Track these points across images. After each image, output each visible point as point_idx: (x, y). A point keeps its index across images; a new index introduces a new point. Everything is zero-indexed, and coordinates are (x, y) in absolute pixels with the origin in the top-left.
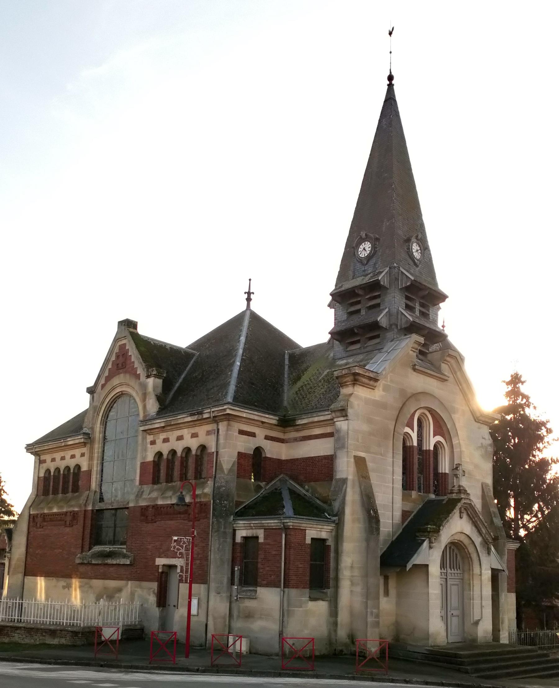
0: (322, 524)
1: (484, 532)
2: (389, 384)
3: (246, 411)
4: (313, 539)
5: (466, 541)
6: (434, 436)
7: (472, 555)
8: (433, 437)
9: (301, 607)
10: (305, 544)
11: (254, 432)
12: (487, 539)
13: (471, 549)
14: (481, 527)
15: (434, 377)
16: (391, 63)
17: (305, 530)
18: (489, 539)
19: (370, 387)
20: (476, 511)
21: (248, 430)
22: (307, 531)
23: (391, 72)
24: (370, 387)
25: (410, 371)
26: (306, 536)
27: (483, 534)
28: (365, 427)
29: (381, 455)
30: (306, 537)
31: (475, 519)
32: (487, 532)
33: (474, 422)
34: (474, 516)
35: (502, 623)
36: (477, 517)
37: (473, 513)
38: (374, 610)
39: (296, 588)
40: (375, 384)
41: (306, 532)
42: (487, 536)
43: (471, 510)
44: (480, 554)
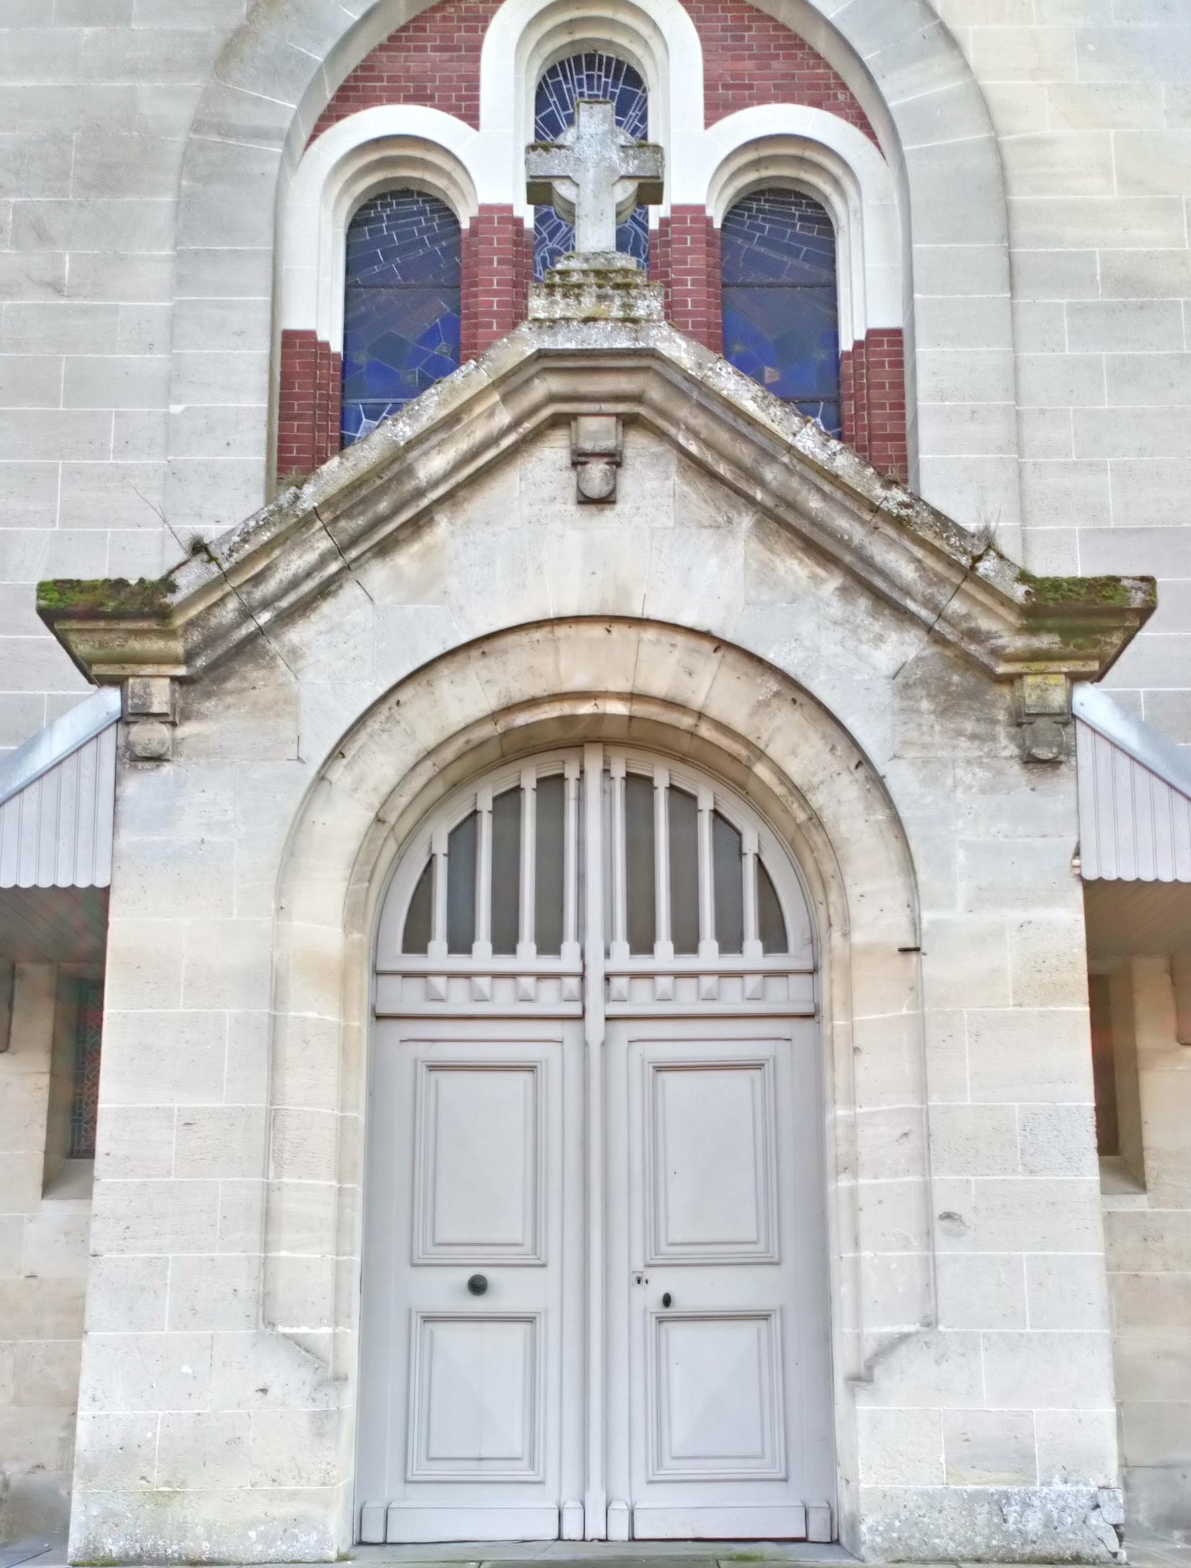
1: (907, 572)
6: (715, 109)
8: (707, 125)
12: (974, 635)
18: (985, 624)
20: (739, 413)
27: (907, 593)
31: (761, 482)
32: (930, 562)
34: (745, 453)
36: (773, 458)
37: (723, 437)
42: (956, 606)
43: (684, 412)
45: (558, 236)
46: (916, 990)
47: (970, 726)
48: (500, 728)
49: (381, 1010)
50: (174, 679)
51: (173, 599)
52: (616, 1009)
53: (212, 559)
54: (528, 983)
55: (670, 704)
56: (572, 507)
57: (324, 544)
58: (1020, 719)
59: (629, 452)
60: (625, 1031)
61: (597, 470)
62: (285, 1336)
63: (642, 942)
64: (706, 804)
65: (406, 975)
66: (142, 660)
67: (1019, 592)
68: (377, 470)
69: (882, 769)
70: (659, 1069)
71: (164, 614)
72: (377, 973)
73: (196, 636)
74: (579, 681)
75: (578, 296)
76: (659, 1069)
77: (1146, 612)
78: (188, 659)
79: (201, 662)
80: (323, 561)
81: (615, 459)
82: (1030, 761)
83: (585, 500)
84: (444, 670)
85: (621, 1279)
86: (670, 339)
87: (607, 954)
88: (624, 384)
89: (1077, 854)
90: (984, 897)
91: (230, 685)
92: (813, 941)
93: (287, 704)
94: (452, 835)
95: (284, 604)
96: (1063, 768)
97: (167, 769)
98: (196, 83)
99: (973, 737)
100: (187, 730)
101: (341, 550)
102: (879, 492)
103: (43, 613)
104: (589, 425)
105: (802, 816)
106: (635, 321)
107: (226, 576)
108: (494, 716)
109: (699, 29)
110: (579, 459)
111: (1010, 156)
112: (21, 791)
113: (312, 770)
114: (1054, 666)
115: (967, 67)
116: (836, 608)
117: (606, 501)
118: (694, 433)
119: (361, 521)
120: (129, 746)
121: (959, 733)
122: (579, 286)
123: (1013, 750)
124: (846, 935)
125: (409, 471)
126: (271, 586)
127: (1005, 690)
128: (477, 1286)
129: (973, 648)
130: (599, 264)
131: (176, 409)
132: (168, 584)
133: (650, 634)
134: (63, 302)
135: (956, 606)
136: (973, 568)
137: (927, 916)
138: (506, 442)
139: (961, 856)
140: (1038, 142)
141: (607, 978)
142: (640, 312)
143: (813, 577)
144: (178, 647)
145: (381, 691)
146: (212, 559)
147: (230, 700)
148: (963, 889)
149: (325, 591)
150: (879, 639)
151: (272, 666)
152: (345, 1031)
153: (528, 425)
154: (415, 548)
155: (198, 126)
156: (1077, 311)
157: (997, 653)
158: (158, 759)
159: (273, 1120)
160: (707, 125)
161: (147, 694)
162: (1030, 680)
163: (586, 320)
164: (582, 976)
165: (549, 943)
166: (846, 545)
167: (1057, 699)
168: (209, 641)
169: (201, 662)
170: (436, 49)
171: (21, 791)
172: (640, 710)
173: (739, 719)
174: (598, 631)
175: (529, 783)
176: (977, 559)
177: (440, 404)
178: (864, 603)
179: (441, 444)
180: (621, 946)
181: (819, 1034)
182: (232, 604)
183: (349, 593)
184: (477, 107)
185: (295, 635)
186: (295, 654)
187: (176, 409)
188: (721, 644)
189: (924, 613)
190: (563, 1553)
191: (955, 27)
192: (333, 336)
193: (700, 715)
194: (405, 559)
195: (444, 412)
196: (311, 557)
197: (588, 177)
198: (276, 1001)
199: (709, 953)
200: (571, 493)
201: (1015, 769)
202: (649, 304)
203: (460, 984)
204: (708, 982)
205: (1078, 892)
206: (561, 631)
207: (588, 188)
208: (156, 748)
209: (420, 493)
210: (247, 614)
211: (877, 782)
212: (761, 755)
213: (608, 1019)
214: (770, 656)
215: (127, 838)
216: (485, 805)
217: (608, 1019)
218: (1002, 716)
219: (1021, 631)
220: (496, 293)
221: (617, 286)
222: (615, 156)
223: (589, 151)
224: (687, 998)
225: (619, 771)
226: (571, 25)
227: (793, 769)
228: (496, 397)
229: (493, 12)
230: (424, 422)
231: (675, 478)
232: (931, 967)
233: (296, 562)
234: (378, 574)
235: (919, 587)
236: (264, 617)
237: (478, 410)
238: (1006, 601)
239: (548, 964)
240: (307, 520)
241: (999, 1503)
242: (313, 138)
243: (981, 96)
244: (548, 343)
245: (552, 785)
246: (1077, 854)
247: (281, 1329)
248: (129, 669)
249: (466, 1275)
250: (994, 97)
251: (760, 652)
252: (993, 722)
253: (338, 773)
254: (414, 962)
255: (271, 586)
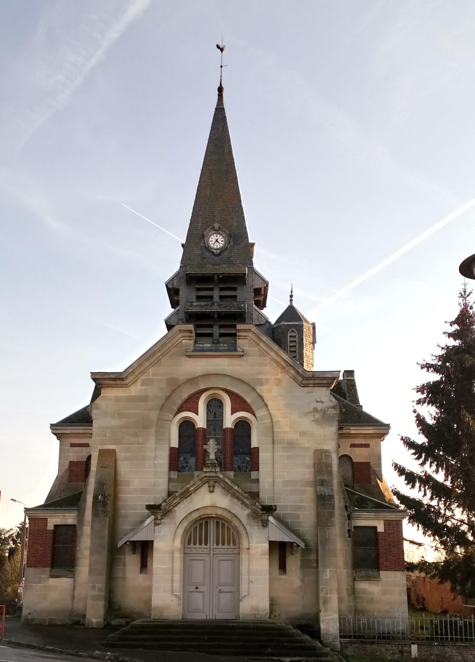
0: (64, 512)
1: (248, 503)
2: (151, 377)
3: (69, 428)
4: (56, 526)
5: (226, 514)
6: (233, 413)
7: (239, 528)
8: (231, 415)
9: (40, 582)
10: (46, 530)
11: (87, 443)
12: (256, 511)
13: (235, 522)
14: (243, 498)
15: (222, 357)
16: (221, 76)
17: (47, 519)
18: (257, 510)
19: (118, 386)
21: (81, 442)
22: (48, 519)
23: (221, 84)
24: (118, 386)
25: (184, 358)
26: (47, 524)
27: (248, 505)
28: (115, 422)
29: (139, 443)
30: (48, 525)
31: (231, 491)
33: (301, 388)
34: (229, 487)
35: (325, 602)
37: (227, 485)
38: (97, 585)
39: (34, 567)
40: (124, 382)
41: (47, 521)
42: (254, 507)
43: (222, 482)
44: (247, 527)
45: (210, 428)
46: (249, 553)
47: (256, 521)
48: (200, 518)
49: (185, 553)
50: (161, 515)
51: (161, 507)
52: (214, 553)
53: (166, 502)
54: (203, 549)
55: (221, 516)
56: (208, 492)
57: (179, 499)
58: (262, 520)
59: (216, 485)
60: (215, 556)
61: (211, 488)
62: (175, 594)
63: (218, 544)
64: (226, 526)
65: (188, 548)
66: (158, 513)
67: (260, 507)
68: (185, 491)
69: (245, 526)
70: (220, 560)
71: (160, 509)
72: (184, 548)
73: (164, 510)
74: (209, 513)
75: (209, 468)
76: (220, 560)
77: (275, 510)
78: (163, 513)
79: (164, 513)
80: (179, 500)
81: (214, 487)
82: (263, 526)
83: (210, 492)
84: (193, 512)
85: (214, 587)
86: (220, 474)
87: (213, 545)
88: (215, 479)
89: (268, 537)
90: (256, 543)
91: (167, 515)
92: (239, 544)
93: (174, 517)
94: (194, 529)
95: (174, 505)
96: (267, 527)
97: (160, 526)
98: (158, 412)
99: (256, 522)
100: (162, 521)
101: (181, 499)
102: (244, 494)
103: (146, 509)
104: (211, 482)
105: (237, 530)
106: (216, 472)
107: (167, 504)
108: (199, 517)
109: (230, 399)
110: (209, 487)
111: (274, 423)
112: (143, 528)
113: (177, 525)
114: (266, 514)
115: (268, 410)
116: (240, 506)
117: (213, 492)
118: (223, 484)
119: (183, 496)
120: (155, 523)
121: (255, 522)
122: (209, 466)
123: (261, 524)
124: (242, 545)
125: (189, 490)
126: (173, 504)
127: (260, 517)
128: (197, 588)
129: (256, 512)
130: (212, 462)
131: (156, 462)
132: (160, 505)
133: (218, 508)
134: (140, 446)
135: (254, 507)
136: (255, 504)
137: (250, 545)
138: (200, 485)
139: (254, 537)
140: (278, 421)
141: (213, 549)
142: (217, 470)
143: (238, 502)
144: (162, 512)
145: (185, 516)
146: (166, 502)
147: (167, 517)
148: (255, 541)
149: (179, 503)
150: (245, 510)
151: (172, 512)
152: (181, 557)
153: (203, 483)
154: (189, 497)
155: (158, 419)
156: (282, 447)
157: (259, 513)
158: (159, 524)
159: (173, 568)
160: (231, 415)
161: (158, 517)
162: (263, 516)
163: (210, 472)
164: (210, 548)
165: (206, 544)
166: (241, 499)
167: (266, 518)
168: (165, 510)
169: (164, 513)
170: (192, 403)
171: (143, 528)
172: (217, 516)
173: (229, 518)
174: (211, 508)
175: (204, 523)
176: (256, 503)
177: (193, 483)
178: (244, 505)
179: (193, 487)
180: (215, 545)
181: (239, 556)
182: (168, 507)
183: (182, 503)
184: (198, 412)
185: (175, 509)
186: (175, 511)
187: (156, 462)
188: (226, 510)
189: (250, 507)
190: (207, 620)
191: (267, 403)
192: (177, 446)
193: (224, 517)
194: (188, 499)
195: (194, 483)
196: (177, 500)
197: (211, 449)
198: (173, 554)
199: (226, 546)
200: (208, 491)
201: (261, 527)
202: (218, 469)
203: (195, 549)
204: (226, 549)
205: (268, 542)
206: (207, 507)
207: (211, 450)
208: (159, 523)
209: (190, 492)
210: (169, 507)
211: (245, 528)
212: (232, 522)
213: (213, 554)
214: (232, 512)
215: (155, 534)
216: (198, 525)
217: (213, 554)
218: (260, 520)
219: (261, 511)
220: (201, 441)
221: (214, 467)
222: (214, 446)
223: (211, 445)
224: (223, 551)
225: (215, 521)
226: (212, 397)
227: (235, 524)
228: (199, 481)
229: (200, 397)
230: (191, 485)
231: (221, 489)
232: (251, 551)
233: (175, 501)
234: (185, 501)
235: (250, 505)
236: (172, 507)
237: (197, 482)
238: (259, 508)
239: (206, 547)
240: (177, 497)
241: (255, 614)
242: (174, 417)
243: (270, 413)
244: (206, 475)
245: (206, 523)
246: (268, 537)
247: (174, 593)
248: (156, 514)
249: (195, 586)
250: (272, 414)
251: (231, 511)
252: (259, 520)
253: (180, 526)
254: (189, 546)
255: (173, 504)
